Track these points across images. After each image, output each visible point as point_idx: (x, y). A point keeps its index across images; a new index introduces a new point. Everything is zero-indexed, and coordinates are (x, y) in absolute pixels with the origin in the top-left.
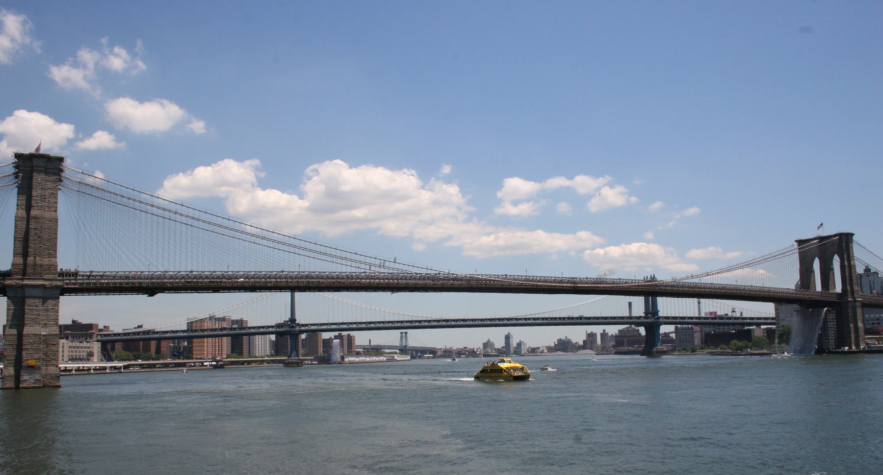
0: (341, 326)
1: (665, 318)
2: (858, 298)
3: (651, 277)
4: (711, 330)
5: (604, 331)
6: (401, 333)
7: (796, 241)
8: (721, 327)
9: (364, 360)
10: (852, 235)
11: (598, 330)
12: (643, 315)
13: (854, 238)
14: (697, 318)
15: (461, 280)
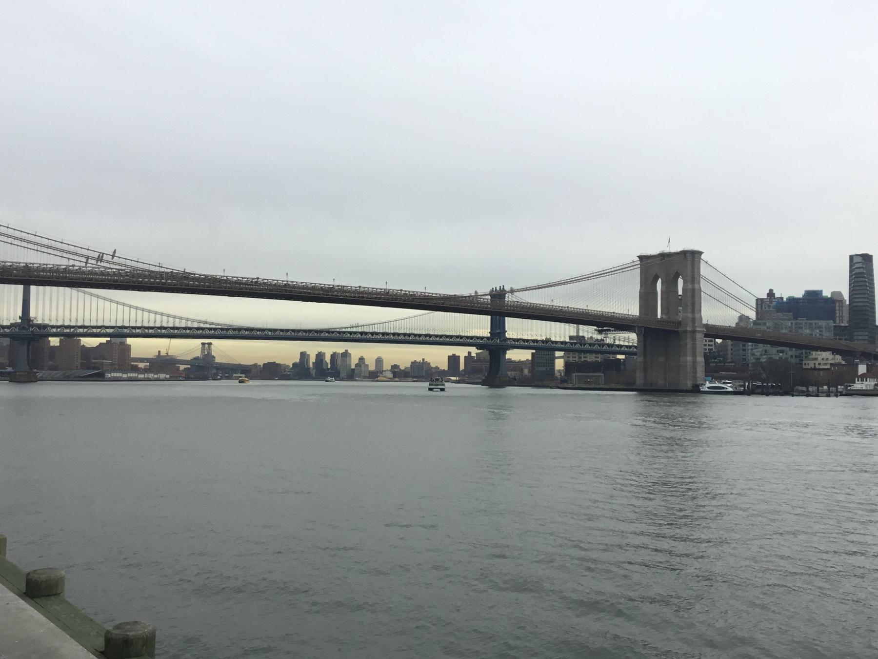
0: (95, 330)
1: (514, 340)
2: (698, 327)
3: (500, 289)
4: (574, 358)
5: (470, 353)
6: (203, 344)
7: (638, 257)
8: (582, 355)
9: (117, 377)
10: (700, 253)
11: (462, 352)
12: (489, 335)
13: (703, 256)
14: (562, 343)
15: (197, 279)
